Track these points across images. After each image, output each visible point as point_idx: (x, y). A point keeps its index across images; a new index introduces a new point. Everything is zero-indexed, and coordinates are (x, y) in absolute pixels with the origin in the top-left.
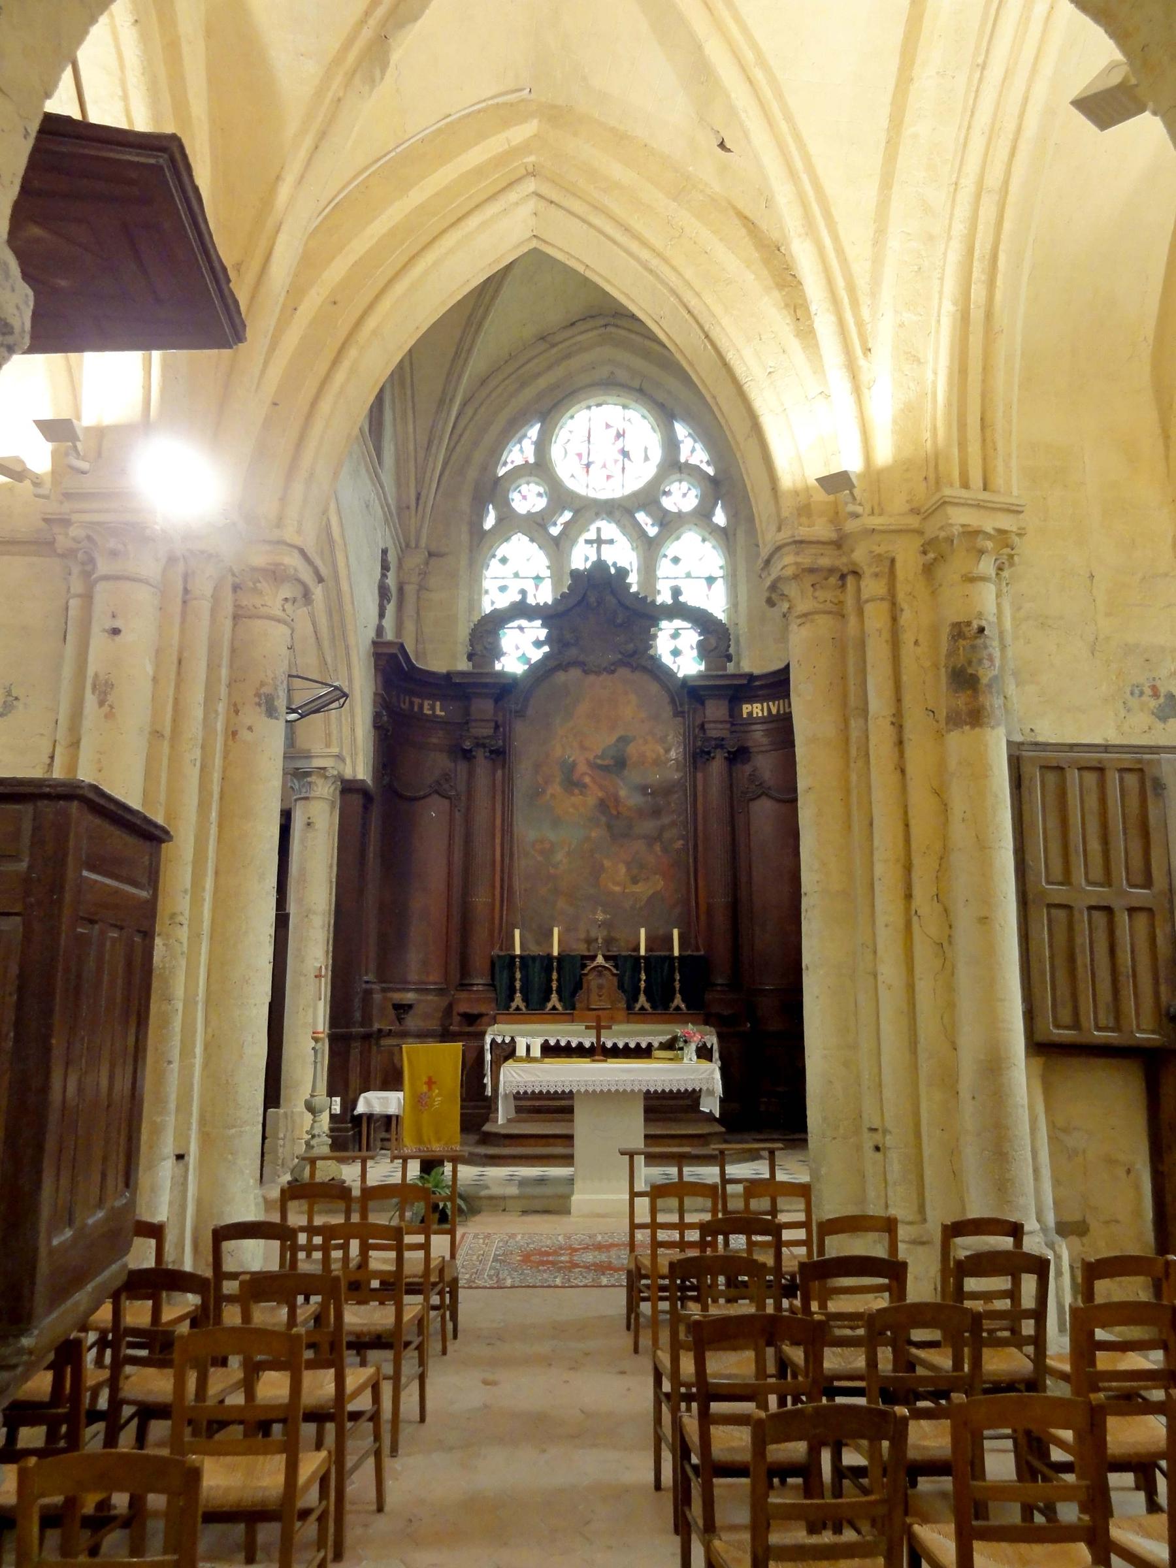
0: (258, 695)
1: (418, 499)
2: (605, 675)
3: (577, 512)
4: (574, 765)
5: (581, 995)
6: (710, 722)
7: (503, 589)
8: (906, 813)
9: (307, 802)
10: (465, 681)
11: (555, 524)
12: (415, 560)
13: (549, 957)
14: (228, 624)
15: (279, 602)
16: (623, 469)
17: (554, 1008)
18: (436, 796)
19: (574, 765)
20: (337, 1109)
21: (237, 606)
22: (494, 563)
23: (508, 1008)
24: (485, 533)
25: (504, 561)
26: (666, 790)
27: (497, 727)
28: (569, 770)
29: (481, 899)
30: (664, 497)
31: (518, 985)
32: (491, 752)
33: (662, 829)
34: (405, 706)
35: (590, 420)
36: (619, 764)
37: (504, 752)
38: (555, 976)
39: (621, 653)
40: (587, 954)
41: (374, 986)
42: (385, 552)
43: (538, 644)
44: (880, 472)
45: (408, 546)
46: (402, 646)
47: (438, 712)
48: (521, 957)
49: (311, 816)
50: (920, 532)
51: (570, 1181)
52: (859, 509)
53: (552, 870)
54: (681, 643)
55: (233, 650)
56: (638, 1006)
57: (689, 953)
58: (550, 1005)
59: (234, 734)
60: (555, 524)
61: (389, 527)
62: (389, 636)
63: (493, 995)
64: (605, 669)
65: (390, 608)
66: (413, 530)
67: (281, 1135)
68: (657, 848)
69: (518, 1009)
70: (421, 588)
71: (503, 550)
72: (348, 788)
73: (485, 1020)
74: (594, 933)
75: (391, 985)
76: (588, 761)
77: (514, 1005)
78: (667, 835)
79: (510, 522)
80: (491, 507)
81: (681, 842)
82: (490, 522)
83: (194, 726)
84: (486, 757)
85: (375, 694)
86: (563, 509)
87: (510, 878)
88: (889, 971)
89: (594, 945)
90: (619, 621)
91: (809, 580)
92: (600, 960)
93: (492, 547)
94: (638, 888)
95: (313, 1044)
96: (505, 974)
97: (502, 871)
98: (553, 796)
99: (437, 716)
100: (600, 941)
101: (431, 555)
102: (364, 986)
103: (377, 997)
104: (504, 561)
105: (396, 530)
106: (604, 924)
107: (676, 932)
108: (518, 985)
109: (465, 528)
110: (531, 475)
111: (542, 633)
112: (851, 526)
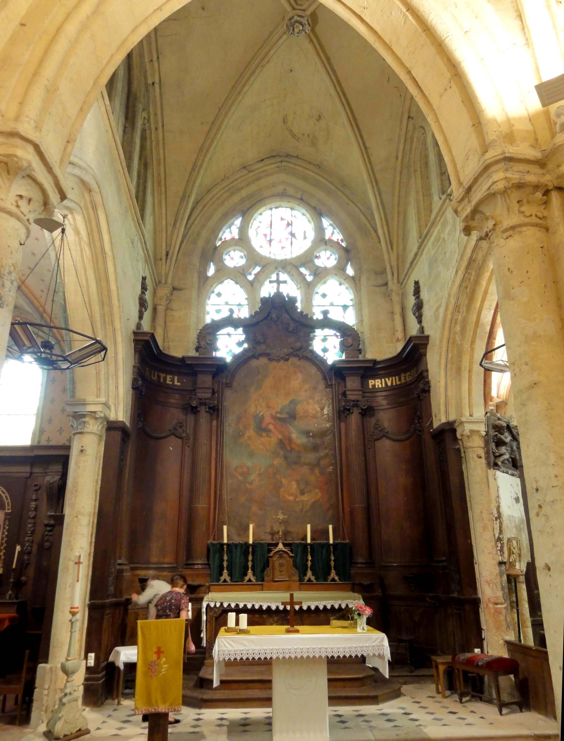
1: (167, 255)
2: (282, 362)
3: (264, 267)
4: (263, 417)
5: (268, 571)
6: (348, 390)
7: (218, 311)
9: (82, 435)
10: (194, 363)
11: (250, 274)
12: (163, 292)
13: (247, 545)
16: (292, 243)
17: (250, 580)
18: (173, 438)
19: (263, 417)
22: (213, 296)
23: (218, 580)
24: (208, 278)
25: (219, 295)
26: (323, 434)
27: (213, 393)
29: (201, 505)
30: (316, 259)
31: (225, 564)
32: (210, 408)
33: (319, 460)
34: (155, 378)
35: (271, 215)
37: (218, 410)
38: (250, 558)
39: (292, 348)
41: (124, 567)
42: (144, 279)
46: (153, 336)
47: (176, 383)
48: (228, 545)
49: (84, 446)
51: (268, 723)
53: (248, 486)
54: (327, 344)
56: (306, 578)
57: (339, 541)
58: (247, 578)
60: (250, 274)
61: (148, 265)
63: (208, 572)
64: (282, 358)
66: (163, 273)
67: (47, 686)
68: (317, 471)
69: (225, 581)
70: (167, 309)
71: (219, 288)
73: (202, 589)
75: (138, 565)
76: (272, 415)
77: (222, 578)
78: (323, 462)
80: (212, 264)
81: (331, 467)
82: (211, 271)
84: (206, 412)
85: (134, 367)
86: (256, 264)
87: (221, 490)
89: (277, 536)
90: (291, 329)
92: (281, 546)
93: (212, 286)
94: (305, 498)
95: (70, 616)
96: (217, 556)
97: (216, 487)
98: (249, 438)
100: (280, 533)
101: (174, 289)
102: (118, 567)
103: (127, 574)
104: (219, 295)
105: (153, 270)
106: (284, 522)
107: (331, 527)
108: (225, 564)
109: (196, 275)
110: (236, 245)
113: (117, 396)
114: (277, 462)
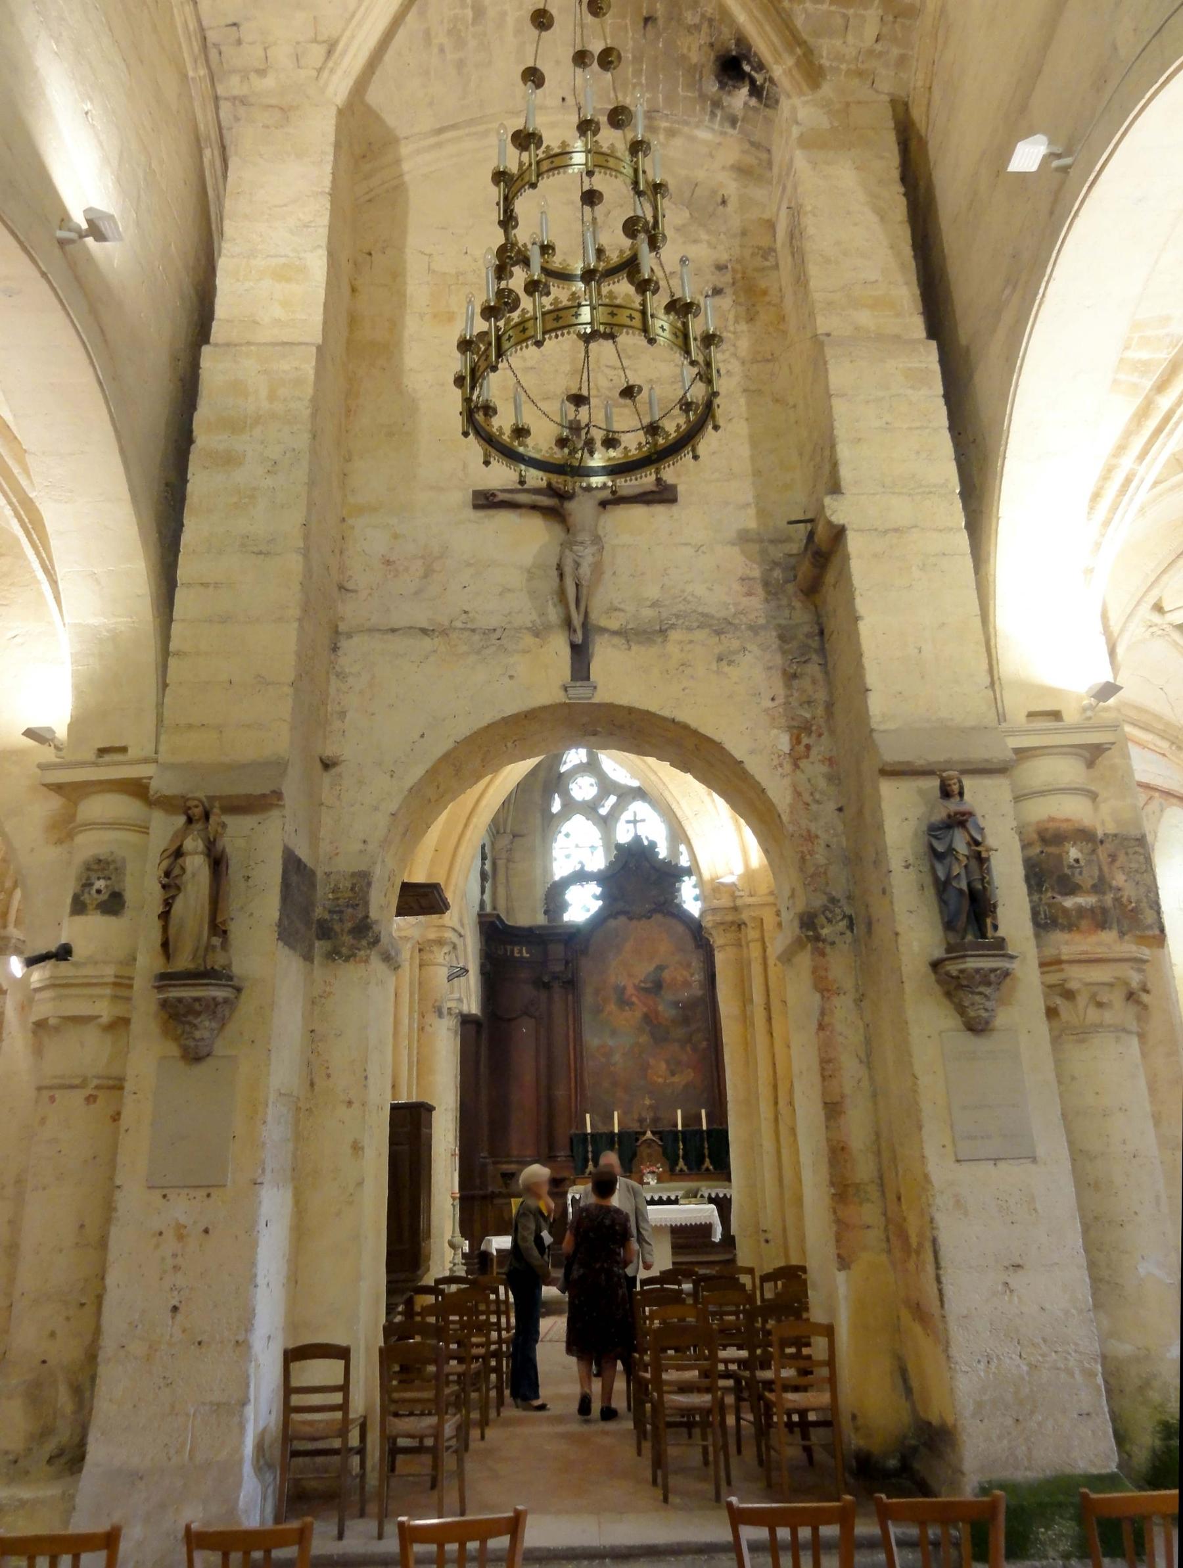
0: (434, 1007)
3: (619, 797)
4: (624, 988)
5: (635, 1161)
7: (568, 856)
8: (774, 1057)
11: (603, 806)
13: (612, 1134)
14: (417, 970)
15: (442, 954)
19: (624, 988)
20: (466, 1249)
21: (421, 960)
22: (560, 837)
24: (553, 816)
25: (567, 835)
27: (567, 963)
28: (621, 991)
29: (560, 1093)
34: (501, 952)
36: (656, 986)
39: (655, 904)
40: (639, 1130)
42: (483, 847)
43: (597, 898)
44: (753, 871)
45: (498, 832)
46: (498, 916)
47: (525, 955)
48: (592, 1135)
50: (775, 904)
52: (742, 893)
53: (612, 1068)
55: (420, 984)
56: (678, 1168)
57: (715, 1126)
59: (423, 1029)
60: (603, 806)
62: (488, 909)
63: (572, 1165)
65: (488, 885)
68: (688, 1049)
70: (508, 860)
71: (566, 827)
72: (466, 1021)
73: (567, 1182)
74: (644, 1114)
75: (499, 1159)
76: (635, 986)
79: (571, 807)
80: (556, 795)
82: (556, 806)
83: (404, 1028)
85: (481, 950)
88: (768, 1144)
91: (722, 927)
92: (649, 1135)
94: (676, 1079)
99: (525, 958)
101: (514, 837)
103: (490, 1168)
104: (567, 835)
106: (651, 1106)
107: (703, 1112)
109: (538, 815)
110: (584, 771)
111: (598, 890)
112: (739, 902)
113: (468, 987)
114: (644, 1039)
